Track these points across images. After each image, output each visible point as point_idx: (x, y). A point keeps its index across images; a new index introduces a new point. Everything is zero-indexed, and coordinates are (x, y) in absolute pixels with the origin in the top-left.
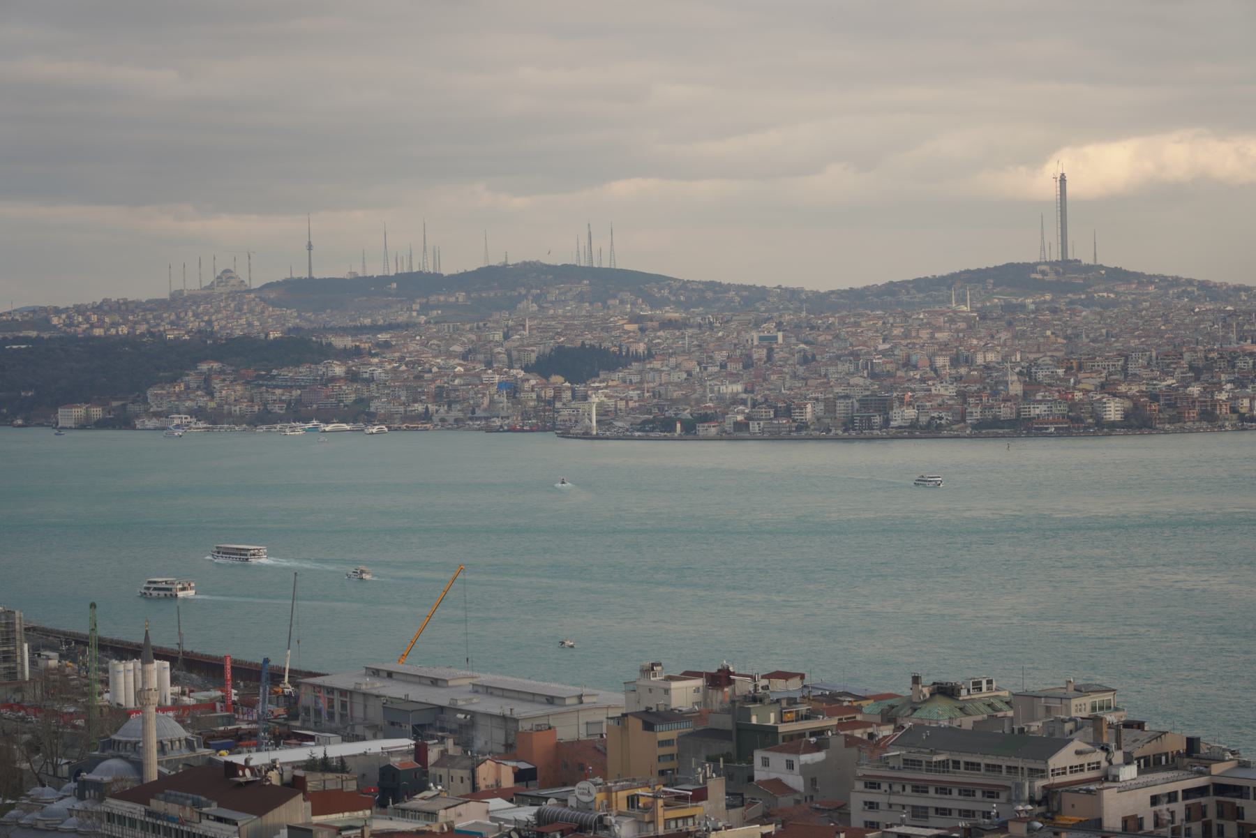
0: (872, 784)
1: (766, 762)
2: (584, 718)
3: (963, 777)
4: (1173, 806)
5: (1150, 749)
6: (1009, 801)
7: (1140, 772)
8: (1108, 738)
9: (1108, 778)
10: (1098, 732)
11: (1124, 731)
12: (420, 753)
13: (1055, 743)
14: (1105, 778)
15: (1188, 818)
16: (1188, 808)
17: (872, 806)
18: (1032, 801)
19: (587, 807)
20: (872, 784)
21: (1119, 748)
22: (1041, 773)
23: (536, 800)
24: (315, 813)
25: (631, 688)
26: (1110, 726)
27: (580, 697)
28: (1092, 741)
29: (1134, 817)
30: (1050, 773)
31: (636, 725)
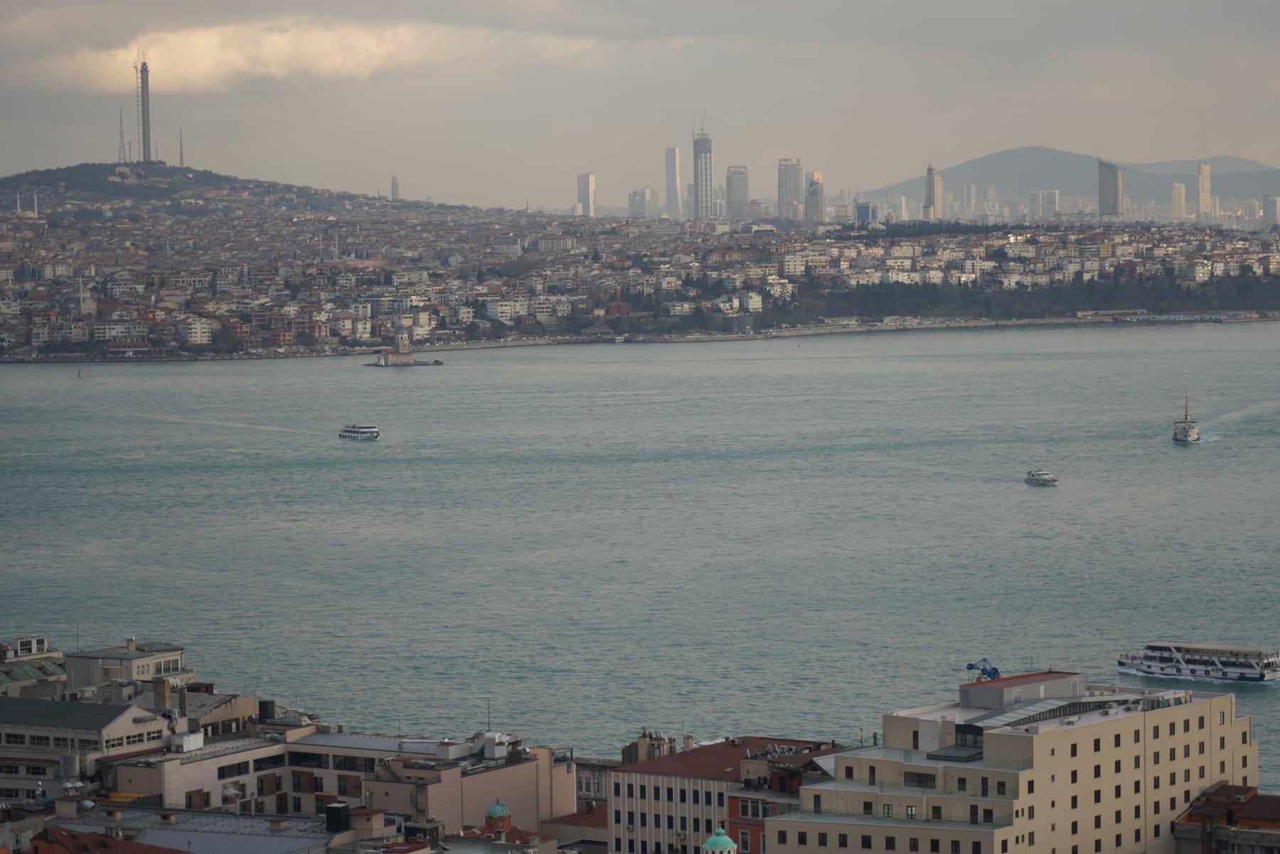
4: (242, 779)
5: (218, 715)
6: (57, 777)
7: (207, 741)
8: (170, 704)
9: (170, 748)
10: (160, 696)
11: (190, 696)
13: (111, 711)
14: (168, 749)
15: (261, 791)
16: (261, 780)
18: (83, 777)
21: (183, 714)
22: (94, 745)
26: (174, 689)
28: (153, 707)
29: (200, 792)
30: (104, 744)
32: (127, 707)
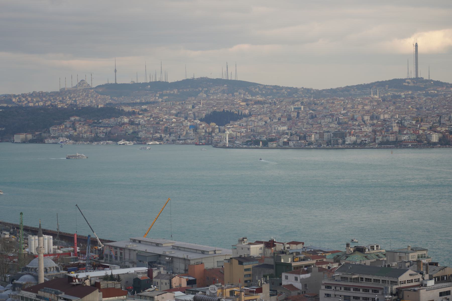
0: (328, 287)
1: (287, 278)
2: (216, 259)
3: (365, 284)
5: (440, 274)
6: (383, 294)
7: (436, 283)
8: (423, 269)
9: (423, 285)
10: (419, 266)
12: (150, 273)
13: (402, 271)
14: (421, 285)
17: (328, 295)
18: (392, 294)
19: (214, 295)
20: (328, 287)
21: (427, 273)
22: (396, 283)
23: (194, 292)
24: (104, 297)
25: (234, 248)
26: (424, 264)
27: (215, 251)
28: (416, 270)
30: (399, 283)
31: (236, 262)
32: (408, 270)
